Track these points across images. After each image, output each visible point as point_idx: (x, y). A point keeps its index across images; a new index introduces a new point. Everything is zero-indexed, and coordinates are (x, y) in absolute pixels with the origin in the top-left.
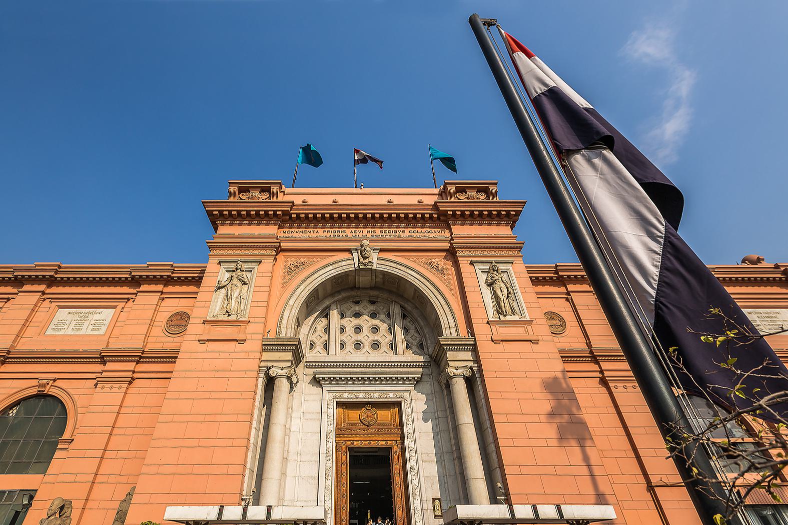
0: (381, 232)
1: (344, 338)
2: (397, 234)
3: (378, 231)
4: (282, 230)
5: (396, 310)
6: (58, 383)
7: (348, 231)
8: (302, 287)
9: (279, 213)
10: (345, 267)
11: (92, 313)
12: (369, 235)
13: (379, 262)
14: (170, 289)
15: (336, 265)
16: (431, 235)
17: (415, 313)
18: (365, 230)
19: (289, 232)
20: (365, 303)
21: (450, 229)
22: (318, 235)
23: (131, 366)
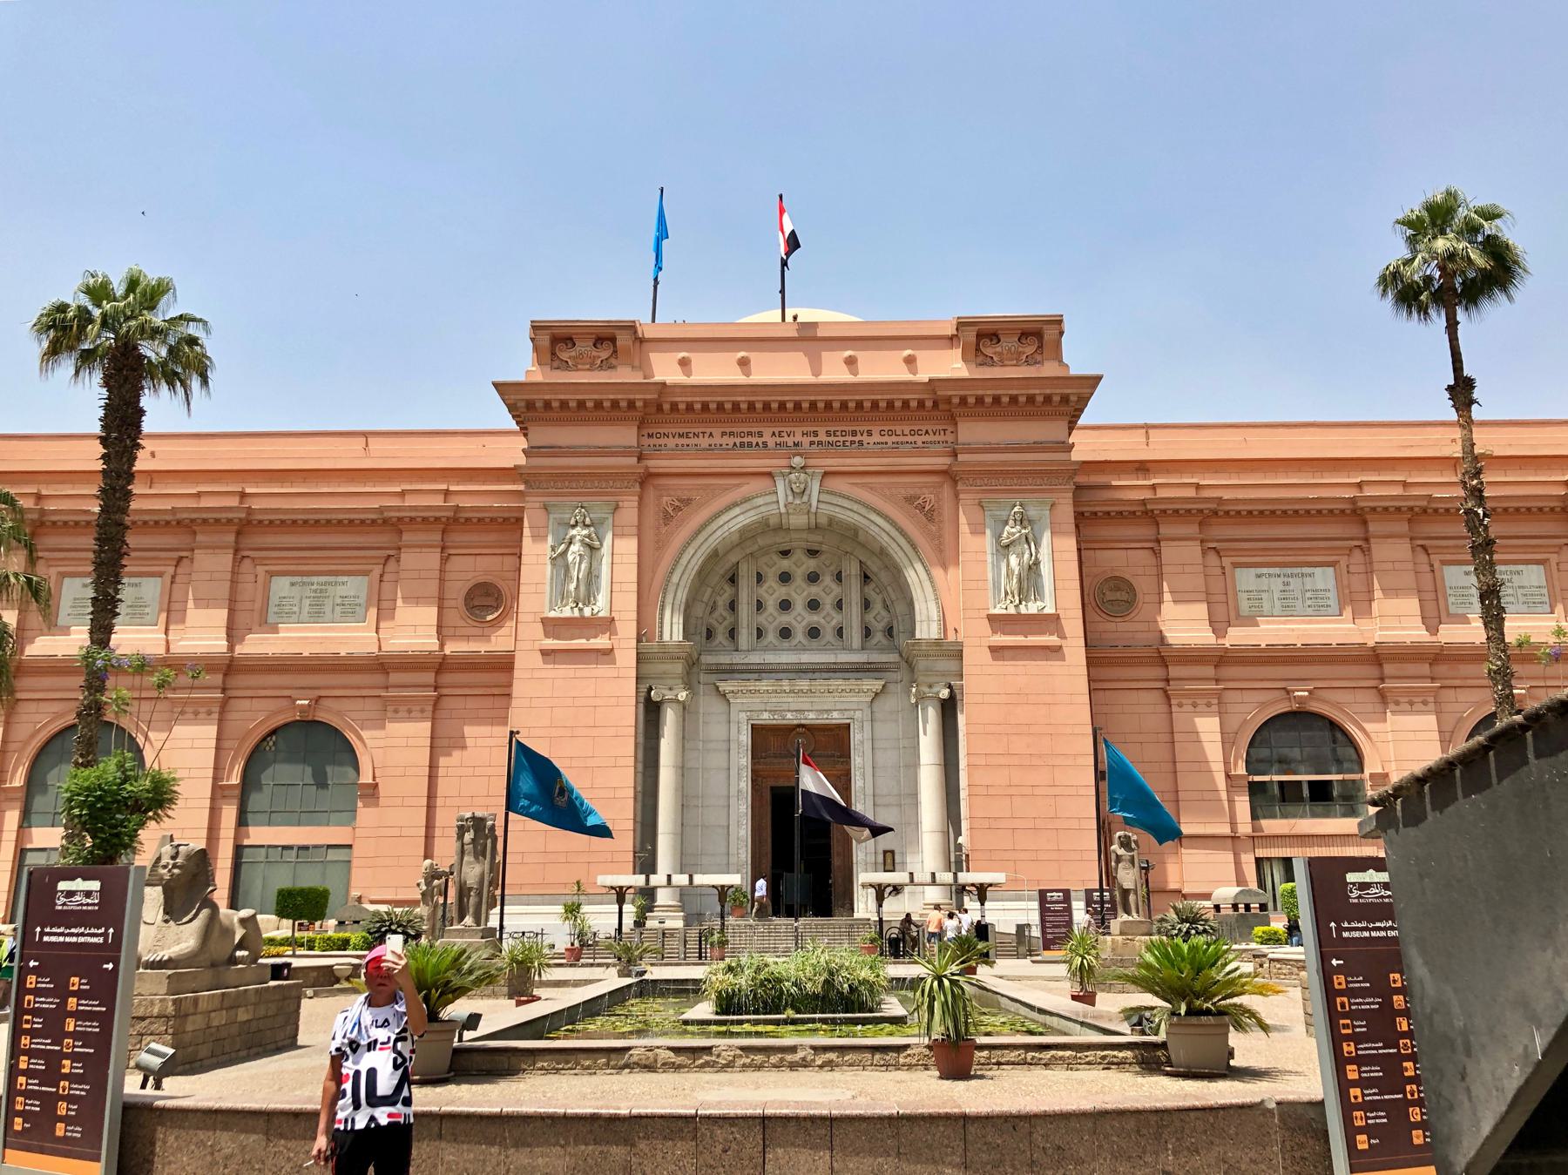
0: (828, 433)
1: (762, 619)
3: (822, 431)
4: (645, 432)
6: (324, 702)
7: (767, 432)
8: (691, 551)
10: (763, 509)
11: (330, 584)
12: (806, 440)
13: (824, 497)
14: (456, 537)
15: (747, 506)
16: (919, 439)
17: (884, 577)
18: (798, 431)
20: (799, 555)
22: (712, 441)
23: (429, 677)
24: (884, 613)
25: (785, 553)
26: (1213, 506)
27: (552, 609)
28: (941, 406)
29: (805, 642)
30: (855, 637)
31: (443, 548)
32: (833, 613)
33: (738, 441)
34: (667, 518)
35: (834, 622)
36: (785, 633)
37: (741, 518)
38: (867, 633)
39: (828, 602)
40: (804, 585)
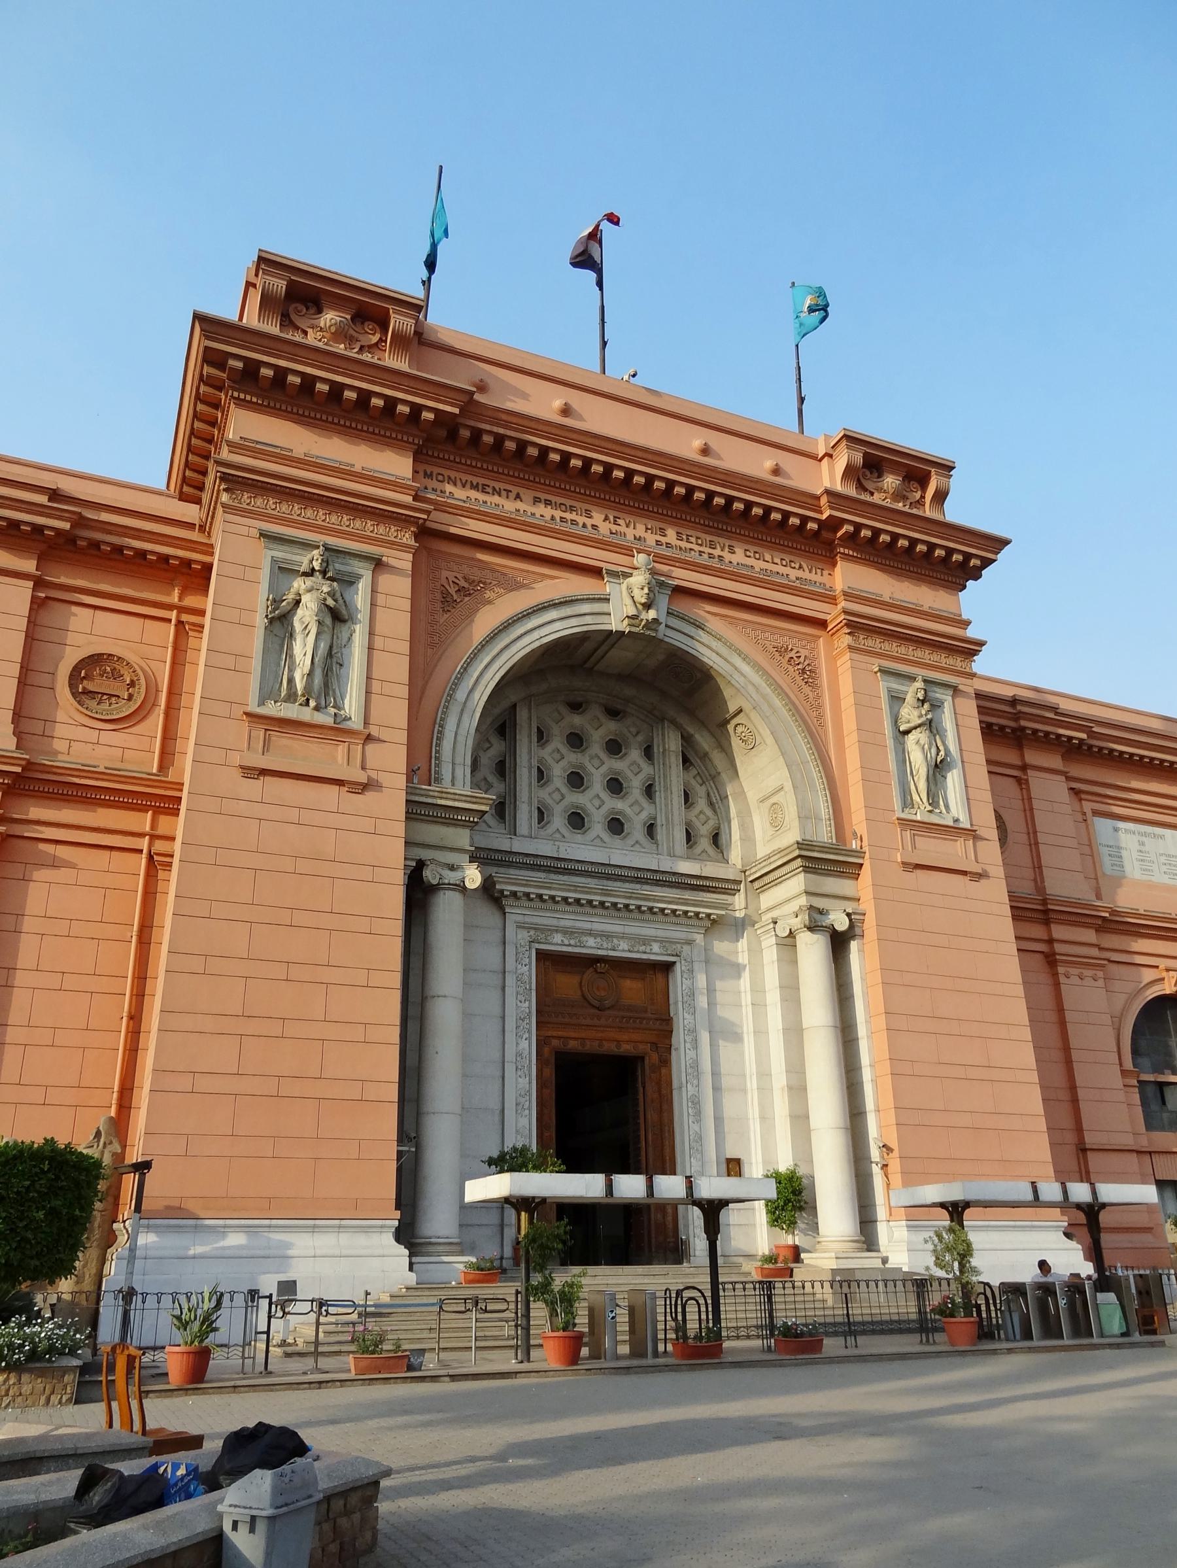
1: (543, 794)
2: (717, 552)
4: (422, 468)
5: (673, 743)
9: (428, 416)
12: (651, 539)
17: (717, 758)
19: (440, 478)
20: (596, 711)
21: (834, 565)
24: (709, 812)
25: (576, 707)
26: (1084, 736)
27: (262, 703)
28: (825, 535)
29: (606, 836)
30: (680, 836)
31: (39, 583)
32: (644, 802)
33: (558, 514)
34: (447, 602)
35: (644, 815)
36: (577, 820)
37: (558, 626)
38: (690, 838)
39: (635, 785)
40: (603, 755)
